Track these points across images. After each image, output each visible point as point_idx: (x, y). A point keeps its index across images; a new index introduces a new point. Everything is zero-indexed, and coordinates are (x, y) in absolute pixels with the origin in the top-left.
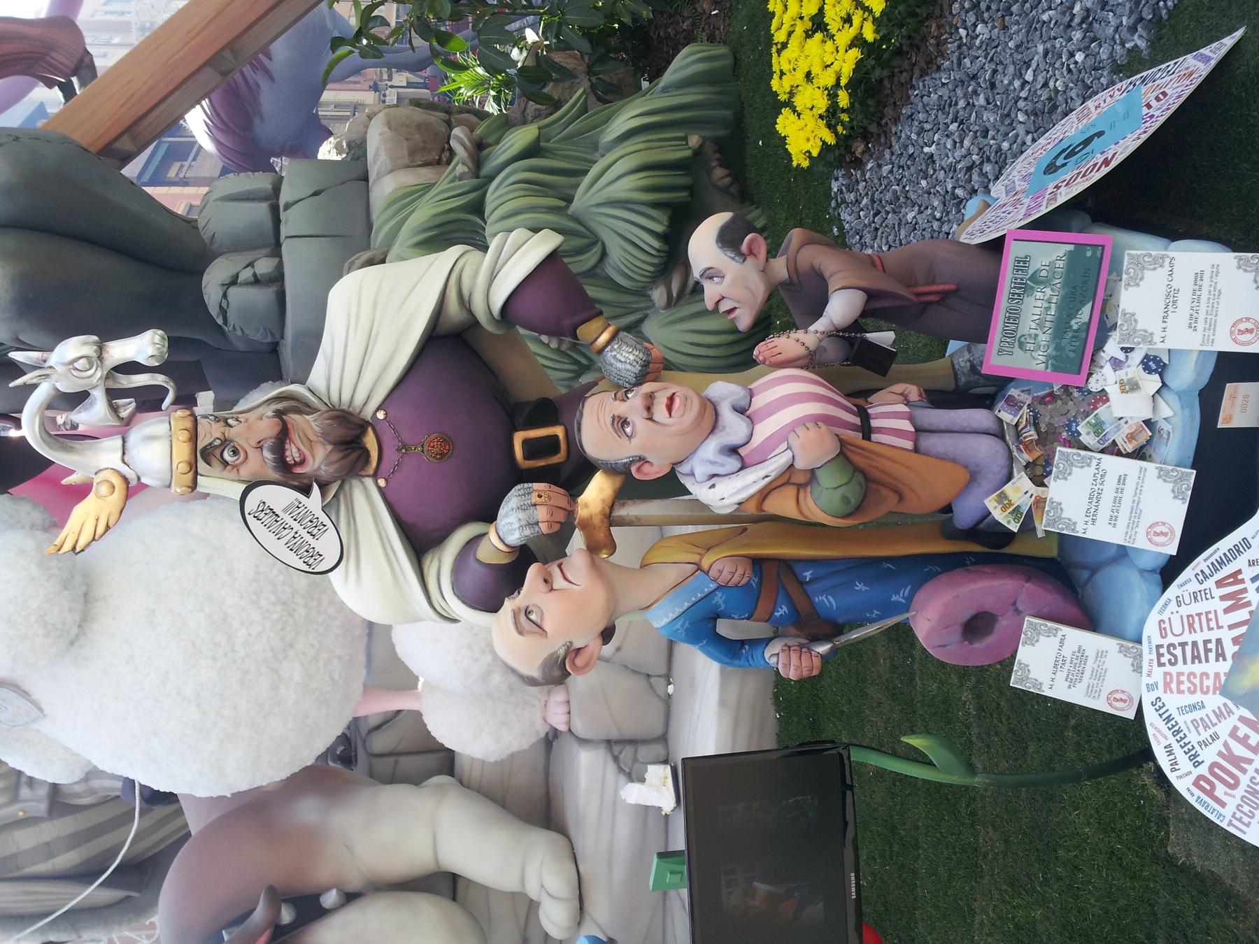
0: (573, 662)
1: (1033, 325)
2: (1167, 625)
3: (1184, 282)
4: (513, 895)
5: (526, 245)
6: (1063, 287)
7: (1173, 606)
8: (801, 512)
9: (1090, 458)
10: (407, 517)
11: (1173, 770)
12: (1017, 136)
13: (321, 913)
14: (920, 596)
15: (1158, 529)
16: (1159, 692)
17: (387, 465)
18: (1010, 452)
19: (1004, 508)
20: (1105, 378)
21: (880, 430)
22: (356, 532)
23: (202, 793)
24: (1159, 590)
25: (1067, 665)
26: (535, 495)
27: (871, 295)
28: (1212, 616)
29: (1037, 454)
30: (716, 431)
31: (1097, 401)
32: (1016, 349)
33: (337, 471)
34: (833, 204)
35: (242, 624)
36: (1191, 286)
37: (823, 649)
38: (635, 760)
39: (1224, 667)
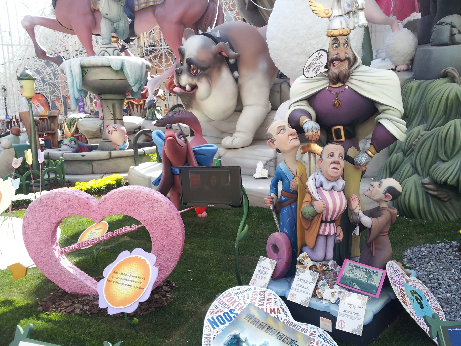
0: (271, 141)
1: (356, 274)
2: (270, 295)
3: (357, 310)
4: (235, 129)
5: (399, 130)
6: (366, 283)
7: (275, 297)
8: (304, 202)
9: (315, 281)
10: (317, 96)
11: (234, 289)
12: (443, 293)
13: (232, 72)
14: (284, 235)
15: (294, 296)
16: (253, 290)
17: (332, 89)
18: (320, 262)
19: (303, 257)
20: (337, 289)
21: (326, 226)
22: (314, 82)
23: (268, 33)
24: (280, 295)
25: (263, 270)
26: (316, 131)
27: (370, 229)
28: (270, 305)
29: (319, 269)
30: (327, 181)
31: (331, 286)
32: (350, 268)
33: (330, 76)
34: (448, 241)
35: (317, 42)
36: (356, 312)
37: (271, 207)
38: (270, 166)
39: (257, 305)
